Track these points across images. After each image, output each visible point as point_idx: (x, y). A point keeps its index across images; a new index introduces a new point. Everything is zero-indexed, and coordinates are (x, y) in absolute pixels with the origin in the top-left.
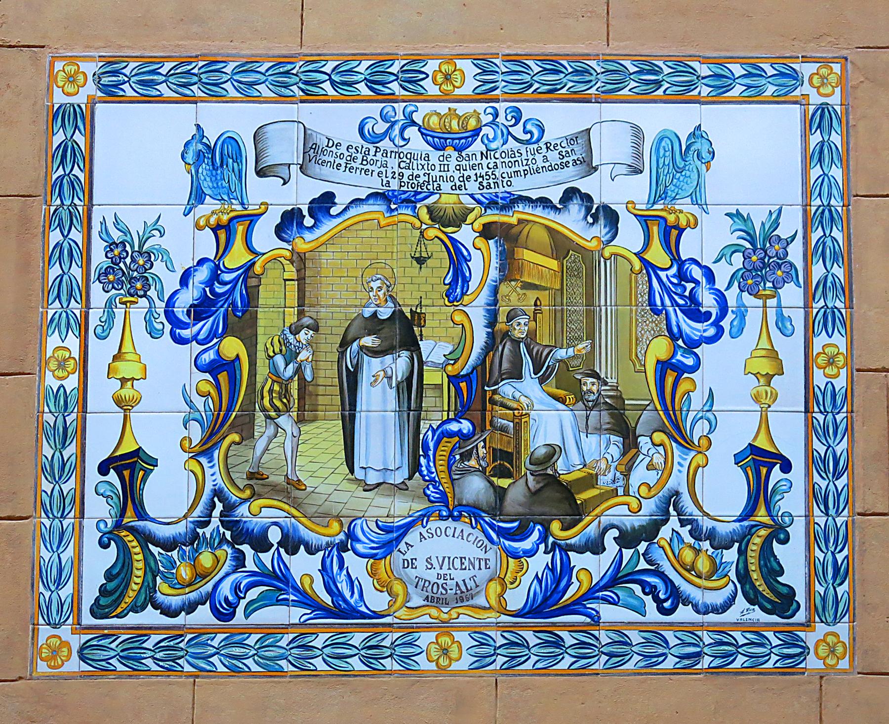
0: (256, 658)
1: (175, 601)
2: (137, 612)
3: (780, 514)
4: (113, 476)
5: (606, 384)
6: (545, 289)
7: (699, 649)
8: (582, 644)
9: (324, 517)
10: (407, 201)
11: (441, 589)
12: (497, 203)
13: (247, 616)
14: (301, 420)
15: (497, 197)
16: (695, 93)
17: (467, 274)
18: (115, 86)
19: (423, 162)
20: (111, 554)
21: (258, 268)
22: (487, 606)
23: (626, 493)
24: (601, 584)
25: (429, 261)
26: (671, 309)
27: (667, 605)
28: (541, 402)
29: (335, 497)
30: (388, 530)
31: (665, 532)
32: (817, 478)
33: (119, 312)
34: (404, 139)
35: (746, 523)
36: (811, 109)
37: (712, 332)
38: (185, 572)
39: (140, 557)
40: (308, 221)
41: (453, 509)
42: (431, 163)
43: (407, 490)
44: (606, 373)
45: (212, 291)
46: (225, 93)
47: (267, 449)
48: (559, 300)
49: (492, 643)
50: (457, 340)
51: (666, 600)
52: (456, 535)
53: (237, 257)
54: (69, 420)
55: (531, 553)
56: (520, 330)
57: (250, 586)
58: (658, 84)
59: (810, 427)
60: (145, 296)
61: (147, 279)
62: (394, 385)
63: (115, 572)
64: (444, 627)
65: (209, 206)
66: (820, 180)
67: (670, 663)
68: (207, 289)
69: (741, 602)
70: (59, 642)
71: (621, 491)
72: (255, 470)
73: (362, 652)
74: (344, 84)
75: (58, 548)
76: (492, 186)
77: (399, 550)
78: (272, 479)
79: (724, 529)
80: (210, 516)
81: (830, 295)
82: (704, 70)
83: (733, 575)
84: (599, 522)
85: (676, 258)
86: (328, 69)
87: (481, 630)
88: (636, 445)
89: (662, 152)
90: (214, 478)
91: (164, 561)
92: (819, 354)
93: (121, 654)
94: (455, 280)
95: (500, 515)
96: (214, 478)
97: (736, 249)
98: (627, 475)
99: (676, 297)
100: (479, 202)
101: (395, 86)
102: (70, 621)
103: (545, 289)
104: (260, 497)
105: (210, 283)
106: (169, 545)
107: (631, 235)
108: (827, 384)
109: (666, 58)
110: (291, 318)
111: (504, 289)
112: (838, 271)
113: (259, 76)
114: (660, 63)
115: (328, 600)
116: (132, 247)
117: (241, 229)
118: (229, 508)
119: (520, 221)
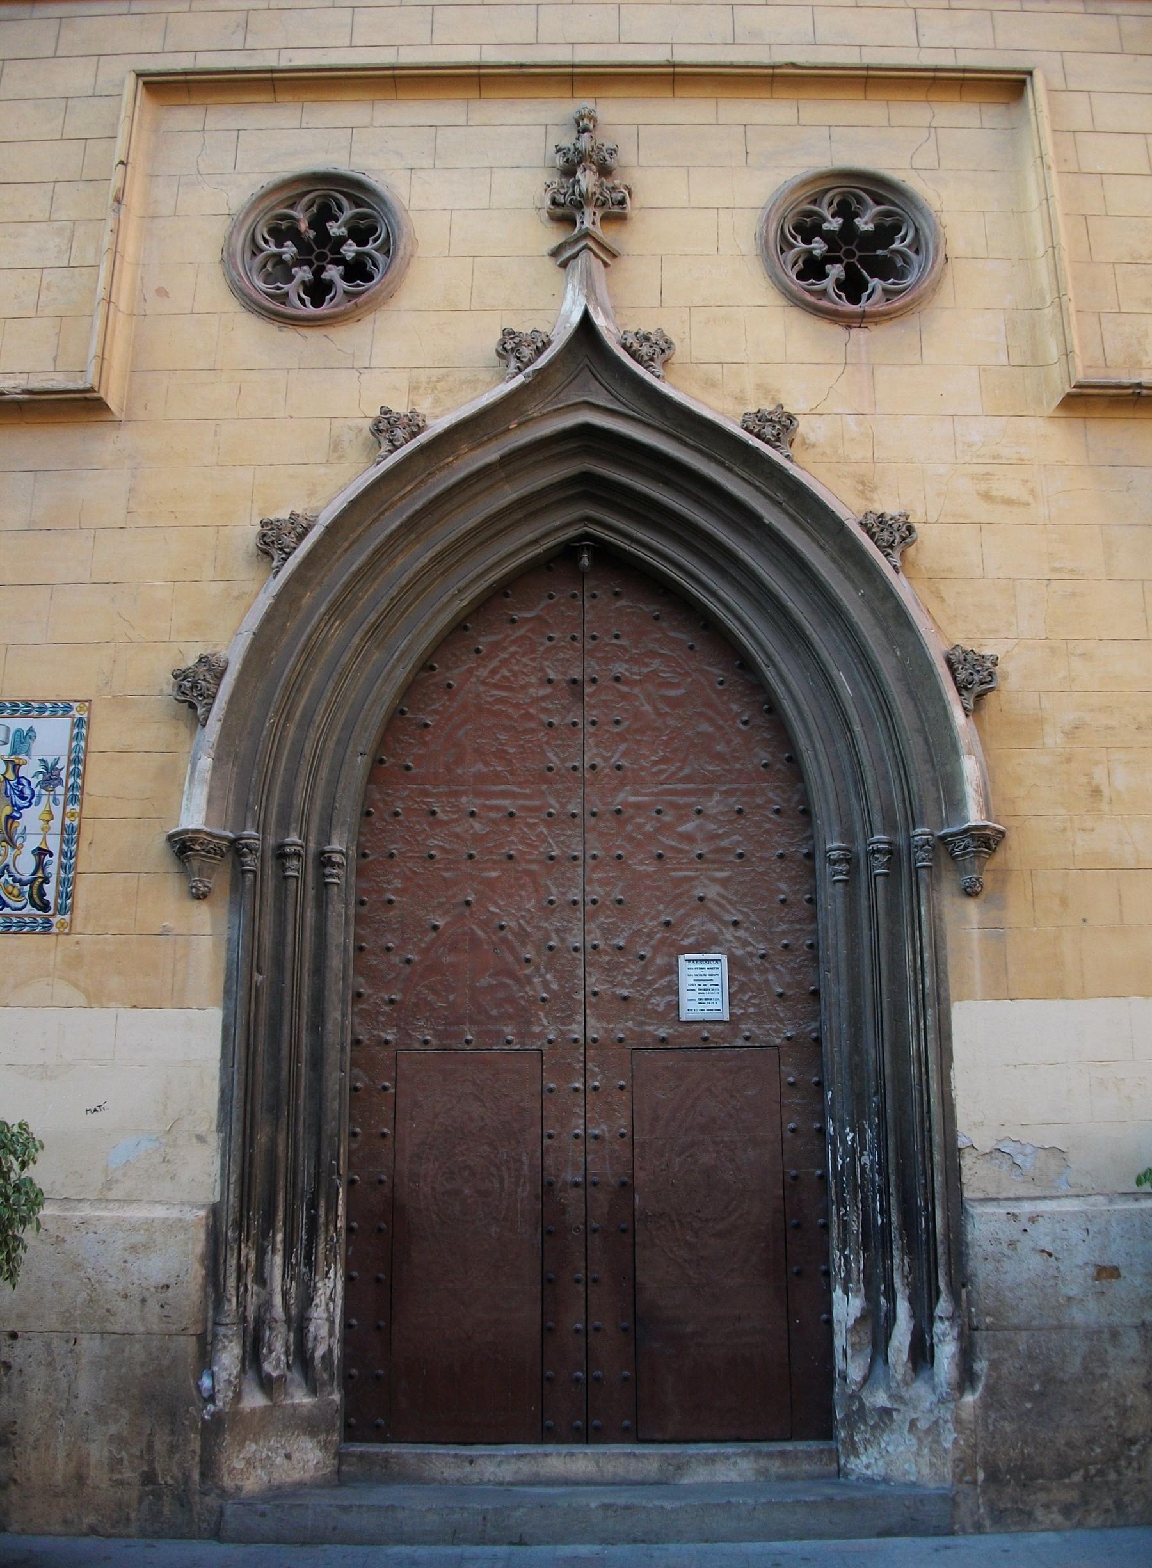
59: (63, 840)
69: (29, 906)
79: (25, 878)
97: (40, 773)
112: (79, 781)
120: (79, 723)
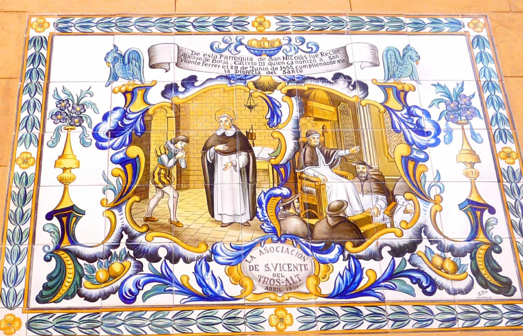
0: (150, 326)
1: (95, 292)
2: (68, 299)
3: (493, 237)
4: (55, 221)
5: (371, 168)
6: (327, 121)
7: (454, 316)
8: (375, 314)
9: (195, 242)
10: (241, 79)
11: (276, 282)
12: (294, 80)
13: (144, 301)
14: (178, 189)
15: (294, 77)
16: (404, 30)
17: (280, 114)
18: (66, 28)
19: (249, 61)
20: (53, 264)
21: (150, 112)
22: (308, 292)
23: (392, 226)
24: (383, 278)
25: (256, 108)
26: (406, 131)
27: (429, 289)
28: (332, 178)
29: (202, 230)
30: (238, 249)
31: (421, 248)
32: (512, 217)
33: (64, 134)
34: (236, 51)
35: (472, 242)
36: (471, 38)
37: (433, 141)
38: (102, 275)
39: (72, 266)
40: (181, 89)
41: (279, 236)
42: (253, 62)
43: (250, 226)
44: (371, 162)
45: (122, 123)
46: (130, 31)
47: (156, 205)
48: (337, 126)
49: (313, 314)
50: (276, 146)
51: (428, 287)
52: (284, 251)
53: (138, 106)
54: (28, 190)
55: (335, 261)
56: (315, 140)
57: (146, 283)
58: (382, 27)
59: (503, 190)
60: (80, 125)
61: (82, 117)
62: (238, 169)
63: (54, 275)
64: (280, 305)
65: (121, 83)
66: (483, 69)
67: (436, 325)
68: (119, 122)
70: (13, 318)
71: (389, 225)
72: (149, 216)
73: (225, 321)
74: (200, 28)
75: (16, 262)
76: (291, 72)
77: (246, 260)
78: (160, 221)
80: (120, 242)
81: (501, 124)
82: (408, 21)
83: (469, 271)
84: (377, 243)
85: (405, 105)
86: (192, 20)
87: (305, 306)
88: (394, 200)
89: (389, 57)
90: (122, 221)
91: (88, 268)
92: (500, 152)
93: (56, 325)
94: (272, 117)
95: (312, 239)
96: (122, 221)
97: (440, 101)
98: (391, 215)
99: (408, 124)
100: (284, 80)
101: (231, 28)
102: (22, 305)
103: (327, 121)
104: (153, 230)
105: (121, 119)
106: (91, 259)
107: (376, 95)
108: (508, 167)
109: (385, 15)
110: (172, 135)
111: (303, 121)
113: (151, 23)
114: (382, 18)
115: (199, 290)
116: (73, 101)
117: (140, 93)
118: (132, 238)
119: (309, 89)
120: (478, 41)
